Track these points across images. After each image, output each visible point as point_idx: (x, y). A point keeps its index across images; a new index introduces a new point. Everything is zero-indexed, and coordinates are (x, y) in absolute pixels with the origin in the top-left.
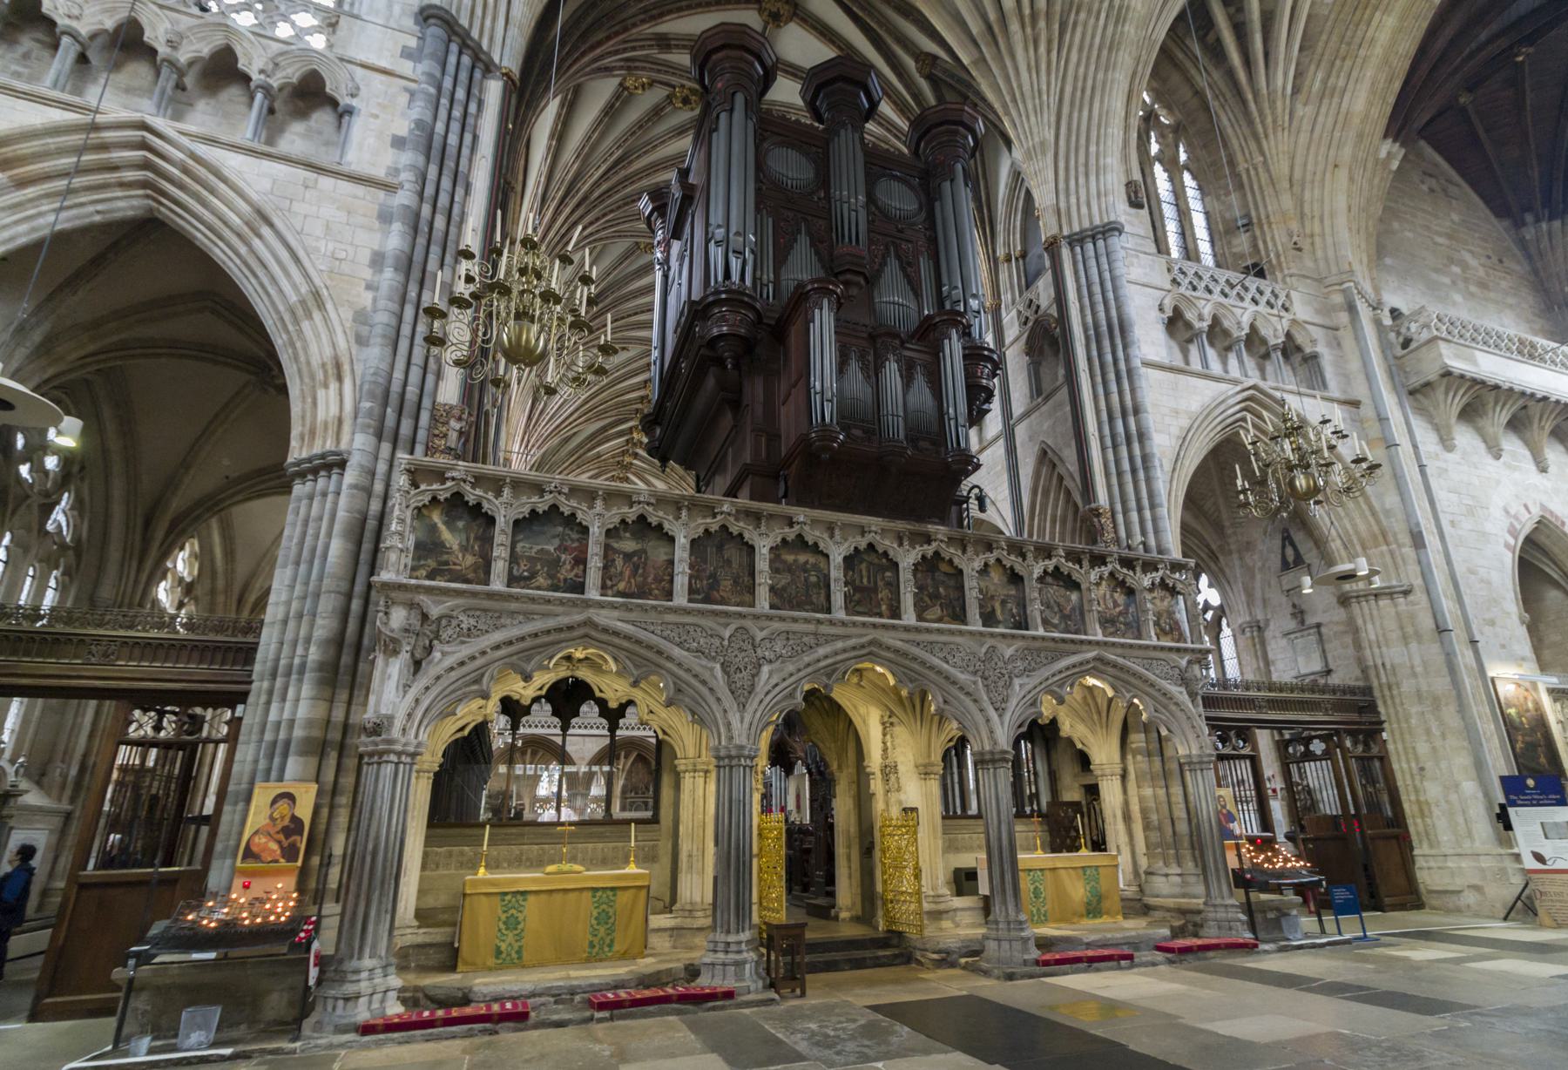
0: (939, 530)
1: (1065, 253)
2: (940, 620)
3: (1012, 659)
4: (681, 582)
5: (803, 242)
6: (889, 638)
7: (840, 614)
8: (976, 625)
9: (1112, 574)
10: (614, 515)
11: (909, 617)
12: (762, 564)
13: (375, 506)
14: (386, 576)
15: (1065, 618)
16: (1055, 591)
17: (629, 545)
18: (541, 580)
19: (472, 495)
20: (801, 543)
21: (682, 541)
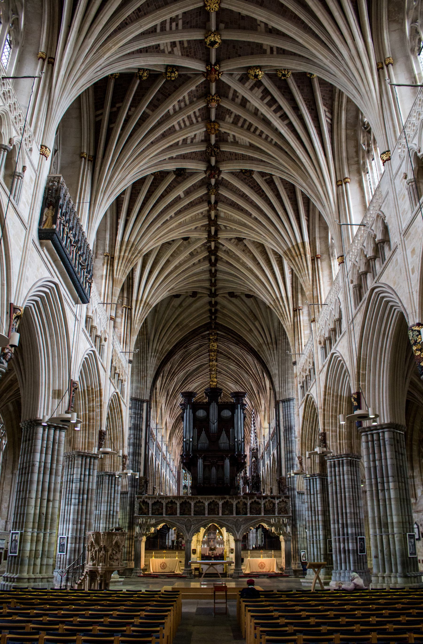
0: (228, 497)
1: (281, 405)
2: (227, 514)
3: (242, 521)
4: (178, 511)
5: (203, 432)
6: (216, 519)
7: (206, 515)
8: (235, 515)
9: (269, 500)
10: (167, 501)
11: (220, 515)
12: (192, 507)
13: (133, 499)
14: (135, 515)
15: (257, 511)
16: (254, 506)
17: (170, 505)
18: (157, 513)
19: (146, 500)
20: (199, 502)
21: (178, 504)
